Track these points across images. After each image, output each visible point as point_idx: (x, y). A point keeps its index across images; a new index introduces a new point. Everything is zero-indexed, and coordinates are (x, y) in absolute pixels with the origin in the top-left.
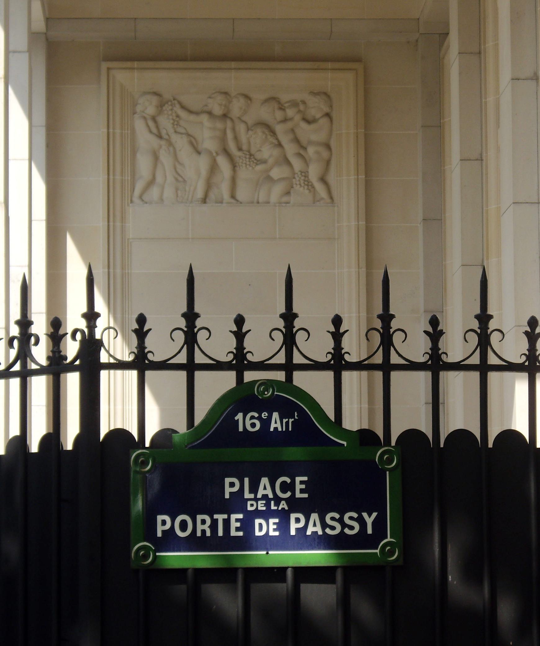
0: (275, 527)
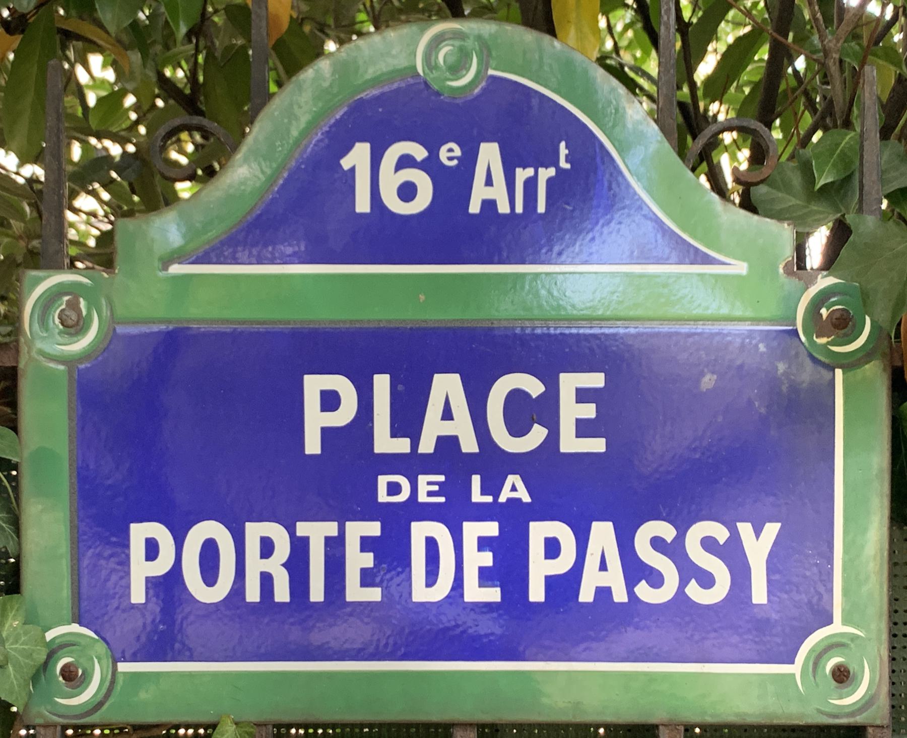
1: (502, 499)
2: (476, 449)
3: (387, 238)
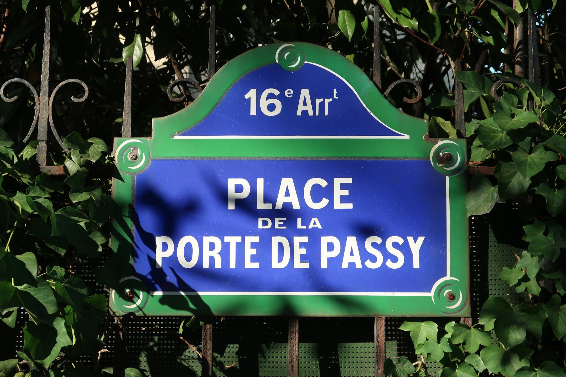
0: (303, 251)
1: (310, 227)
2: (299, 208)
3: (262, 125)
